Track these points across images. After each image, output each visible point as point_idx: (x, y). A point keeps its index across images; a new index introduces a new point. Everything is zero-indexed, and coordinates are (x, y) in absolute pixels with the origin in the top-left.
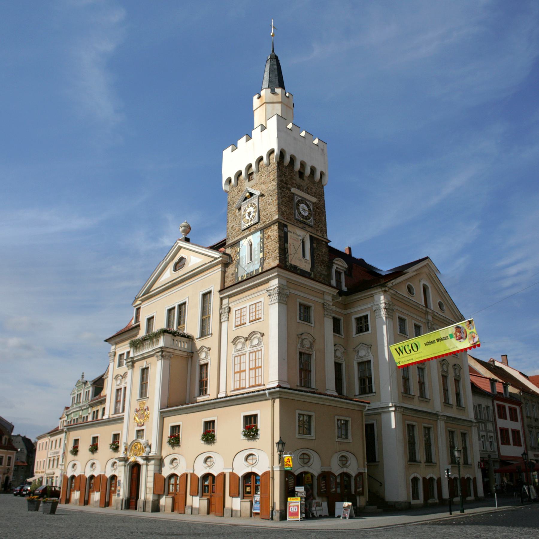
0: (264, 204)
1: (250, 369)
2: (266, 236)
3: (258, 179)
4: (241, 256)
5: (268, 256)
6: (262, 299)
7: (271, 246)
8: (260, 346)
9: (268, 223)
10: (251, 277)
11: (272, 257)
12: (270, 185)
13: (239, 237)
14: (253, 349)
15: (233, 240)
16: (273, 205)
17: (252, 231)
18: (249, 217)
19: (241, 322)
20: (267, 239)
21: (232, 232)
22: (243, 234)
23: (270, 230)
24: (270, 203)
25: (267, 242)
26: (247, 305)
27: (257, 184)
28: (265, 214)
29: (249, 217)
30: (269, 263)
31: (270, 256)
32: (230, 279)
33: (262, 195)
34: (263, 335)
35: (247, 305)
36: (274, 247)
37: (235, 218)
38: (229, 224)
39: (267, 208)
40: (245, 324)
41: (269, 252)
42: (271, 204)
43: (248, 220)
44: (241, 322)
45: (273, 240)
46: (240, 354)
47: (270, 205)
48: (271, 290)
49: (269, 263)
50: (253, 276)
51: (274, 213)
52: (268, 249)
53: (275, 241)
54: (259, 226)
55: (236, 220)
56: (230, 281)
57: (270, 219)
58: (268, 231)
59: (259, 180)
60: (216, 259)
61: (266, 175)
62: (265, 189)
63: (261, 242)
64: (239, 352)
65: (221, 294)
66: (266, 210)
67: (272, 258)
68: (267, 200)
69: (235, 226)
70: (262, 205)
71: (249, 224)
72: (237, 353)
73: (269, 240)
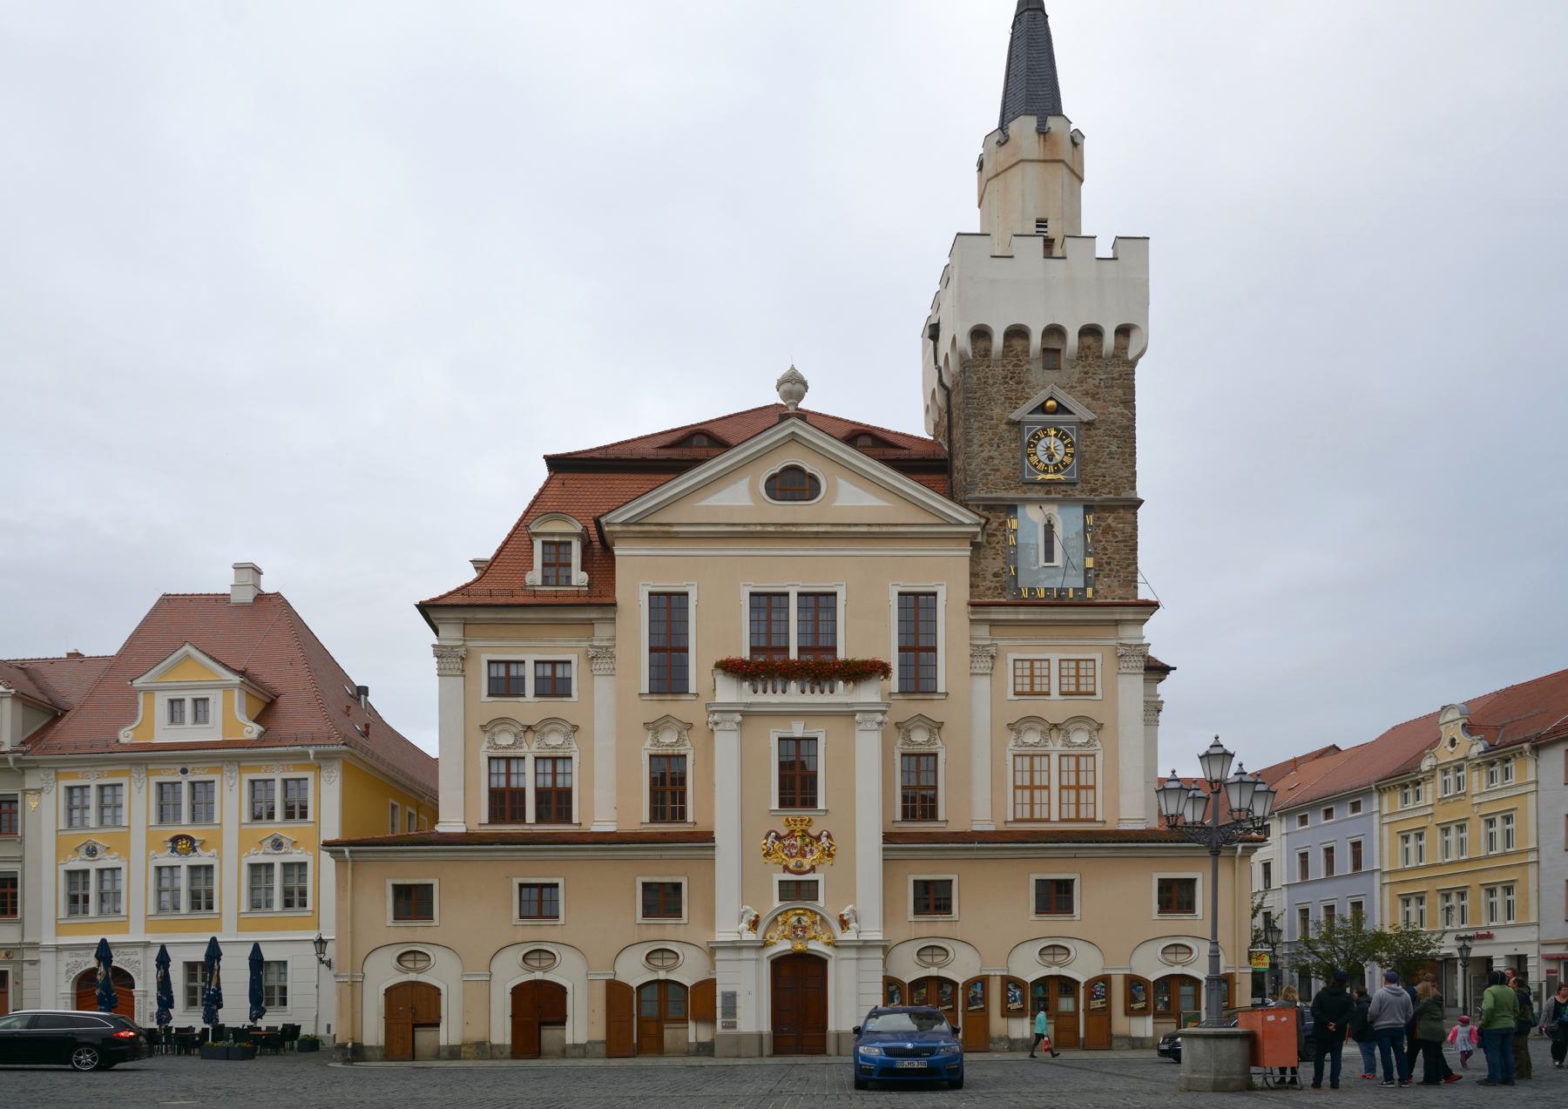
0: (1094, 447)
1: (1061, 787)
2: (1103, 524)
3: (1076, 377)
4: (1019, 541)
5: (1107, 572)
6: (1098, 656)
7: (1117, 551)
8: (1091, 748)
9: (1105, 496)
10: (1059, 600)
11: (1119, 576)
12: (1112, 409)
13: (1012, 494)
14: (1071, 749)
15: (992, 492)
16: (1123, 462)
17: (1053, 496)
18: (1051, 460)
19: (1032, 687)
20: (1105, 532)
21: (987, 471)
22: (1025, 493)
23: (1112, 515)
24: (1110, 453)
25: (1101, 538)
26: (1054, 657)
27: (1072, 387)
28: (1098, 472)
29: (1051, 460)
30: (1109, 586)
31: (1113, 573)
32: (987, 583)
33: (1090, 424)
34: (1100, 727)
35: (1054, 657)
36: (1123, 556)
37: (996, 440)
38: (975, 448)
39: (1104, 462)
40: (1048, 694)
41: (1109, 564)
42: (1117, 457)
43: (1047, 465)
44: (1032, 687)
45: (1122, 541)
46: (1031, 753)
47: (1114, 458)
48: (1130, 646)
49: (1109, 586)
50: (1066, 601)
51: (1126, 481)
52: (1106, 554)
53: (1127, 546)
54: (1077, 493)
55: (999, 447)
56: (989, 588)
57: (1113, 491)
58: (1107, 515)
59: (1081, 381)
60: (962, 524)
61: (1101, 380)
62: (1099, 411)
63: (1085, 531)
64: (1028, 748)
65: (972, 613)
66: (1099, 464)
67: (1117, 578)
68: (1105, 441)
69: (996, 462)
70: (1086, 446)
71: (1049, 477)
72: (1024, 748)
73: (1110, 537)
